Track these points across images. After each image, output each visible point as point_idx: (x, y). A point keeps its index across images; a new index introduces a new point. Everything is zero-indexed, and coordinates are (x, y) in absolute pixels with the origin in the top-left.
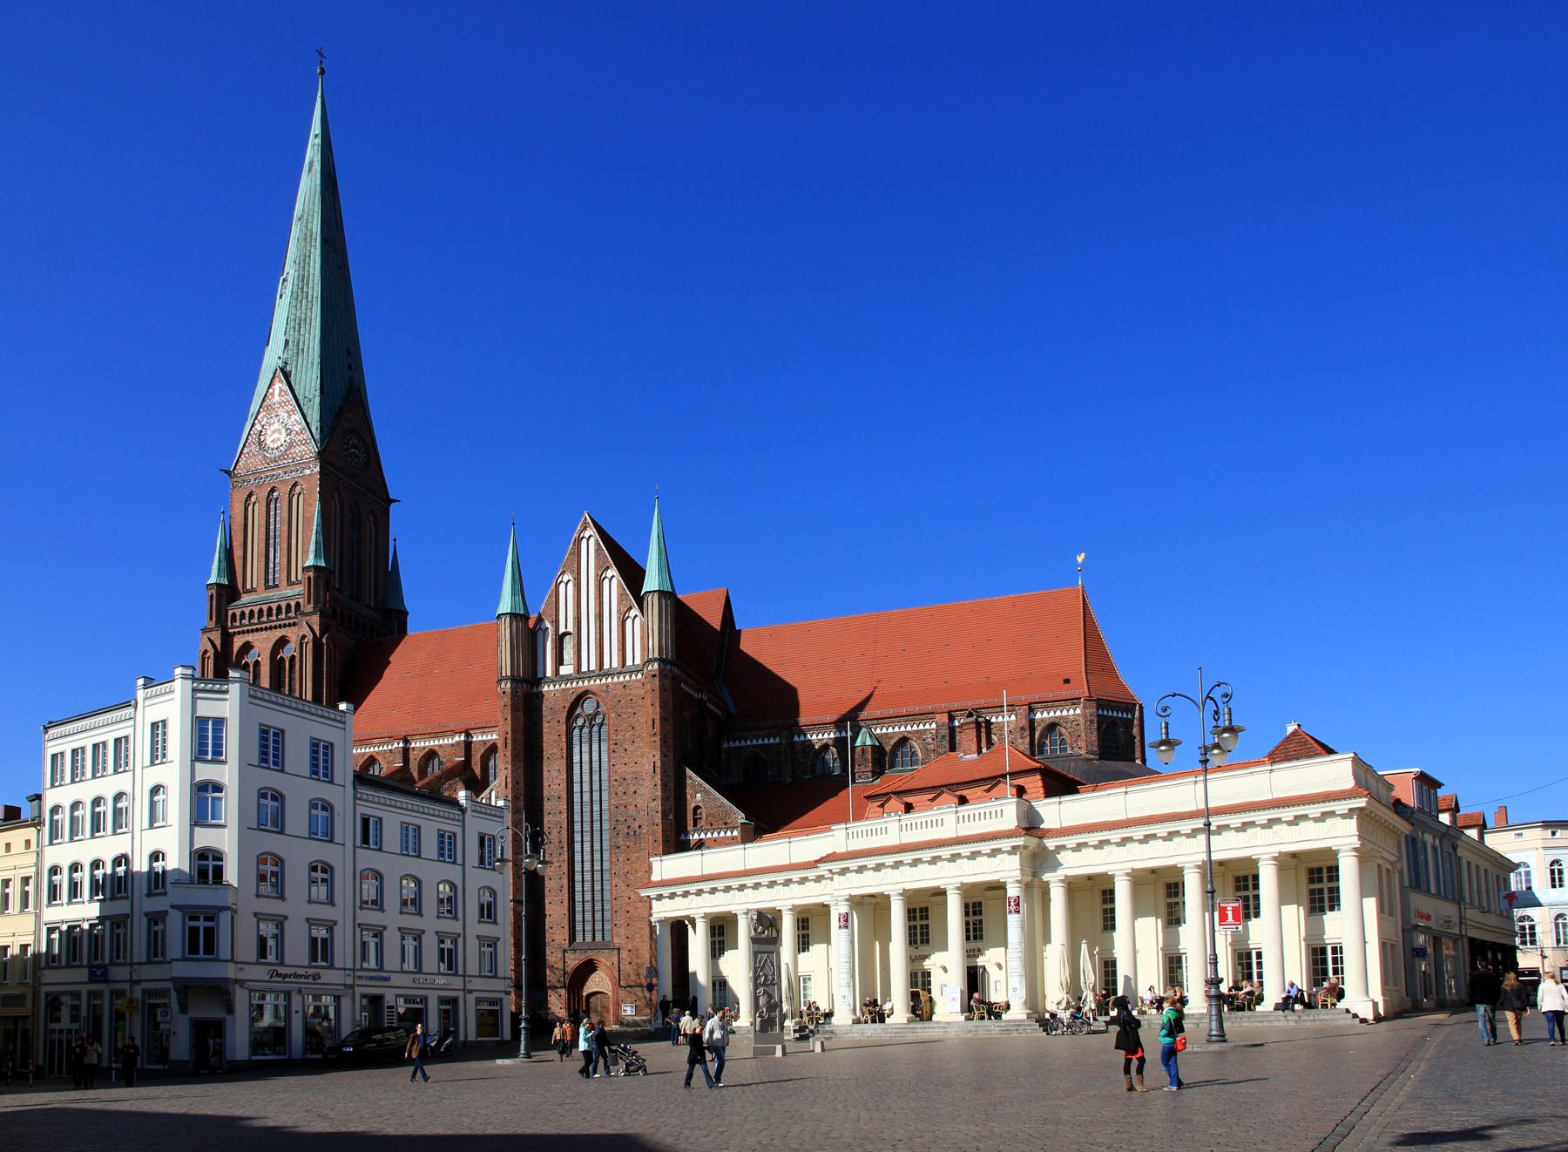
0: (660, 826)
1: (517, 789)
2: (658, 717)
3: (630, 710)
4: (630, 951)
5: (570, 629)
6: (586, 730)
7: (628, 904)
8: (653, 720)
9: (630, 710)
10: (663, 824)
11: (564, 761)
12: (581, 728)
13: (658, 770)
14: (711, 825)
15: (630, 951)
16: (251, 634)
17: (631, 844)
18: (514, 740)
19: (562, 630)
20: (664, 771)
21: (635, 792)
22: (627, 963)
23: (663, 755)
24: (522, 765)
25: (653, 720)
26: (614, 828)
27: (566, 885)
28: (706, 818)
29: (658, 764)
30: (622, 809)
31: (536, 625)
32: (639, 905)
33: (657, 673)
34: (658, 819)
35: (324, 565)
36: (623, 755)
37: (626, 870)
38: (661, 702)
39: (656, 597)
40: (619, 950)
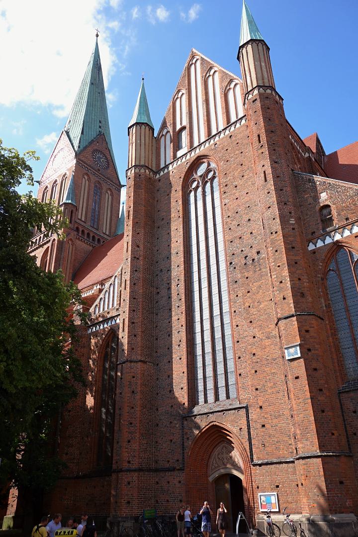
0: (280, 232)
2: (263, 130)
3: (237, 152)
4: (261, 407)
6: (200, 190)
7: (253, 344)
8: (259, 136)
9: (237, 152)
10: (283, 229)
11: (181, 219)
13: (270, 177)
14: (347, 219)
15: (261, 407)
17: (250, 274)
19: (178, 127)
20: (276, 177)
21: (249, 220)
22: (259, 426)
23: (274, 162)
25: (259, 136)
26: (231, 263)
27: (184, 339)
28: (339, 215)
29: (269, 171)
30: (237, 241)
31: (159, 134)
32: (267, 342)
33: (258, 97)
34: (277, 225)
35: (70, 202)
36: (234, 191)
37: (247, 305)
38: (264, 118)
39: (249, 46)
40: (246, 408)
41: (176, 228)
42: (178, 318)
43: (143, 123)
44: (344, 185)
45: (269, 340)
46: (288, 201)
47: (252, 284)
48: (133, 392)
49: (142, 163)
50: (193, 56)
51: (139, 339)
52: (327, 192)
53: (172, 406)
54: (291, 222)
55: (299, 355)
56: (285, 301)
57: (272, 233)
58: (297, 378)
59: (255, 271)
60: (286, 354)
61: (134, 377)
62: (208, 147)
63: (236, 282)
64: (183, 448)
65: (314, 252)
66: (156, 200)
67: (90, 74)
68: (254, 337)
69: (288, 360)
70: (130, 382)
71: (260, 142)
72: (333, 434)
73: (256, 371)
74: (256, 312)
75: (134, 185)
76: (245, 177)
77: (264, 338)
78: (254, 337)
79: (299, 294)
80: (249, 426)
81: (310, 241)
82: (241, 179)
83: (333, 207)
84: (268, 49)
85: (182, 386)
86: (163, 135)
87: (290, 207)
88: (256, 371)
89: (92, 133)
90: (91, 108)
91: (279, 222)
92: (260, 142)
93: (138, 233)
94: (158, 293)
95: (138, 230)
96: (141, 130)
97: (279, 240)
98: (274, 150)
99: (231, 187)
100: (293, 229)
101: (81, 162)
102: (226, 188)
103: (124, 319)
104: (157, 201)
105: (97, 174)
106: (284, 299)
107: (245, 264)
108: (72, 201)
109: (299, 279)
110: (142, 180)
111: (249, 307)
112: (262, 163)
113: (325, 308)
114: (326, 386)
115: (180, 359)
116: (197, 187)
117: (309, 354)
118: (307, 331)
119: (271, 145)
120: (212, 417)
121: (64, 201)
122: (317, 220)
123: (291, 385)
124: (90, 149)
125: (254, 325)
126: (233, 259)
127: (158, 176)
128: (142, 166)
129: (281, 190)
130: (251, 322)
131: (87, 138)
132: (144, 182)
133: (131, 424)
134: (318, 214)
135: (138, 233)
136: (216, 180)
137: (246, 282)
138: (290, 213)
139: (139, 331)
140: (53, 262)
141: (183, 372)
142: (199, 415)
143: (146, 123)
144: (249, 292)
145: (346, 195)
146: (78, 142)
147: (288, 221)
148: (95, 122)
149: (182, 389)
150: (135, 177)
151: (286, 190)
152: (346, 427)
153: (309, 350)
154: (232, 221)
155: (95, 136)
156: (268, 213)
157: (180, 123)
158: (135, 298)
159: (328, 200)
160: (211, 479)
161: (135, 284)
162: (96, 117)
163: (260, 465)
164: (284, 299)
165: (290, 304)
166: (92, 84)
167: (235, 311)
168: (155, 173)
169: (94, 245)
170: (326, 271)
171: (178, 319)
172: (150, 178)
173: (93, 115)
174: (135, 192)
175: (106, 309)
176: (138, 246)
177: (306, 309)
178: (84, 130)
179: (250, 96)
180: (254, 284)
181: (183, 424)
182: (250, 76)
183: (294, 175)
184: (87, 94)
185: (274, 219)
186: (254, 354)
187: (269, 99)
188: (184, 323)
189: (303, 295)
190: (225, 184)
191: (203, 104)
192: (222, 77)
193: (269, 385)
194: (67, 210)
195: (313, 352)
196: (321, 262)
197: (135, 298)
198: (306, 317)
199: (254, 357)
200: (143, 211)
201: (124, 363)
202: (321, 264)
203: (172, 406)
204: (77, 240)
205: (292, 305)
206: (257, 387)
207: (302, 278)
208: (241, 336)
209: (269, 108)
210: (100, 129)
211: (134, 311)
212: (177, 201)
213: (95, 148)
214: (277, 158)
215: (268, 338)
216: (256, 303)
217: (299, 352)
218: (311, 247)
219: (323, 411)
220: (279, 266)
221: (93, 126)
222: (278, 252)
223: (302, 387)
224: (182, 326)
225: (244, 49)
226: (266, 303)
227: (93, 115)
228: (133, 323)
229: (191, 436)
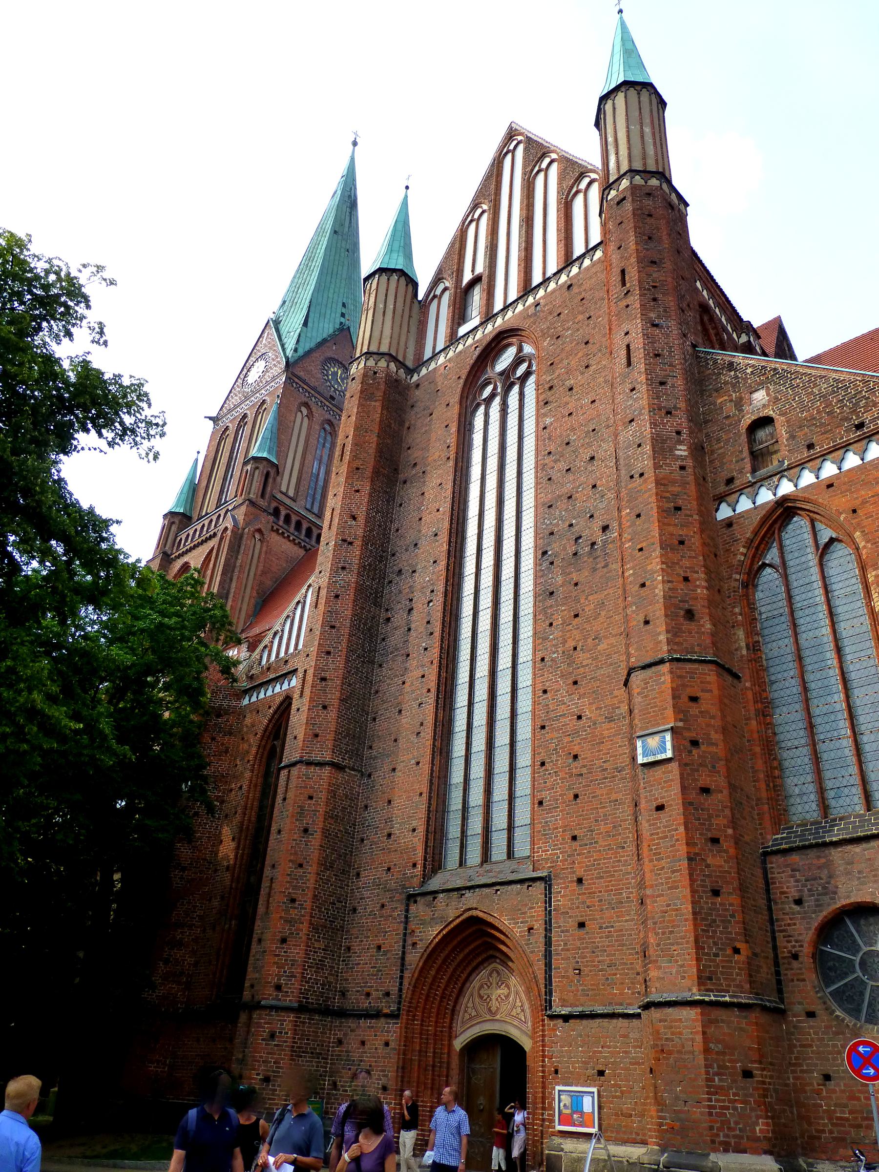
1: (351, 527)
2: (633, 260)
4: (580, 881)
5: (479, 269)
6: (497, 401)
8: (623, 272)
9: (580, 317)
10: (656, 466)
11: (451, 463)
12: (489, 401)
13: (638, 356)
16: (189, 554)
18: (355, 444)
21: (592, 458)
22: (572, 923)
24: (367, 489)
25: (623, 272)
28: (792, 437)
30: (562, 504)
31: (427, 295)
32: (607, 730)
33: (628, 194)
35: (265, 455)
37: (571, 644)
41: (439, 481)
42: (422, 673)
43: (394, 271)
44: (809, 371)
45: (612, 724)
46: (675, 408)
47: (586, 599)
48: (306, 831)
49: (384, 349)
50: (511, 137)
51: (332, 714)
52: (768, 389)
53: (389, 869)
54: (677, 453)
55: (669, 754)
56: (648, 627)
57: (632, 477)
58: (660, 808)
59: (595, 570)
60: (639, 750)
61: (311, 798)
62: (520, 312)
63: (552, 593)
64: (403, 965)
65: (729, 523)
66: (407, 425)
67: (333, 214)
68: (579, 717)
69: (643, 765)
70: (302, 808)
71: (624, 284)
72: (737, 951)
73: (576, 796)
74: (590, 661)
75: (362, 392)
76: (592, 368)
77: (601, 719)
78: (579, 717)
79: (682, 613)
80: (548, 924)
81: (720, 499)
82: (582, 374)
83: (779, 420)
84: (663, 104)
85: (414, 823)
86: (435, 296)
87: (681, 420)
88: (576, 796)
89: (326, 325)
90: (329, 278)
91: (650, 453)
92: (624, 284)
93: (358, 491)
94: (388, 620)
95: (358, 485)
96: (388, 284)
97: (646, 492)
98: (655, 300)
99: (559, 391)
100: (682, 468)
101: (296, 380)
102: (549, 393)
103: (305, 671)
104: (409, 428)
105: (328, 407)
106: (647, 622)
107: (575, 554)
108: (269, 452)
109: (686, 579)
110: (379, 383)
111: (575, 649)
112: (625, 327)
113: (744, 652)
114: (730, 831)
115: (418, 763)
116: (493, 396)
117: (694, 752)
118: (694, 699)
119: (649, 289)
120: (471, 899)
121: (254, 452)
122: (741, 451)
123: (645, 826)
124: (318, 356)
125: (582, 691)
126: (549, 544)
127: (415, 377)
128: (383, 354)
129: (662, 383)
130: (575, 683)
131: (314, 334)
132: (382, 387)
133: (293, 901)
134: (744, 438)
135: (358, 491)
136: (532, 379)
137: (574, 594)
138: (678, 433)
139: (333, 696)
140: (220, 573)
141: (421, 794)
142: (443, 891)
143: (401, 271)
144: (576, 616)
145: (812, 393)
146: (294, 341)
147: (672, 450)
148: (334, 305)
149: (414, 830)
150: (365, 375)
151: (673, 386)
152: (774, 939)
153: (695, 743)
154: (555, 461)
155: (331, 331)
156: (628, 434)
157: (470, 269)
158: (333, 627)
159: (768, 405)
160: (458, 1044)
161: (337, 596)
162: (336, 298)
163: (566, 1018)
164: (647, 622)
165: (659, 634)
166: (335, 232)
167: (543, 659)
168: (410, 372)
169: (308, 547)
170: (756, 567)
171: (423, 676)
172: (396, 380)
173: (332, 291)
174: (360, 405)
175: (282, 654)
176: (354, 518)
177: (696, 649)
178: (310, 320)
179: (613, 193)
180: (590, 598)
181: (407, 911)
182: (617, 154)
183: (698, 357)
184: (323, 250)
185: (639, 445)
186: (576, 757)
187: (654, 197)
188: (433, 686)
189: (690, 615)
190: (549, 385)
191: (521, 226)
192: (565, 170)
193: (603, 828)
194: (257, 472)
195: (703, 748)
196: (744, 547)
197: (333, 627)
198: (696, 666)
199: (576, 764)
200: (374, 446)
201: (294, 764)
202: (742, 550)
203: (389, 869)
204: (274, 535)
205: (663, 638)
206: (576, 833)
207: (693, 576)
208: (552, 715)
209: (650, 215)
210: (342, 320)
211: (328, 653)
212: (446, 426)
213: (329, 354)
214: (659, 317)
215: (610, 719)
216: (590, 640)
217: (669, 745)
218: (724, 512)
219: (716, 893)
220: (641, 550)
221: (328, 312)
222: (643, 517)
223: (669, 831)
224: (429, 691)
225: (610, 102)
226: (613, 640)
227: (332, 291)
228: (323, 679)
229: (420, 940)
